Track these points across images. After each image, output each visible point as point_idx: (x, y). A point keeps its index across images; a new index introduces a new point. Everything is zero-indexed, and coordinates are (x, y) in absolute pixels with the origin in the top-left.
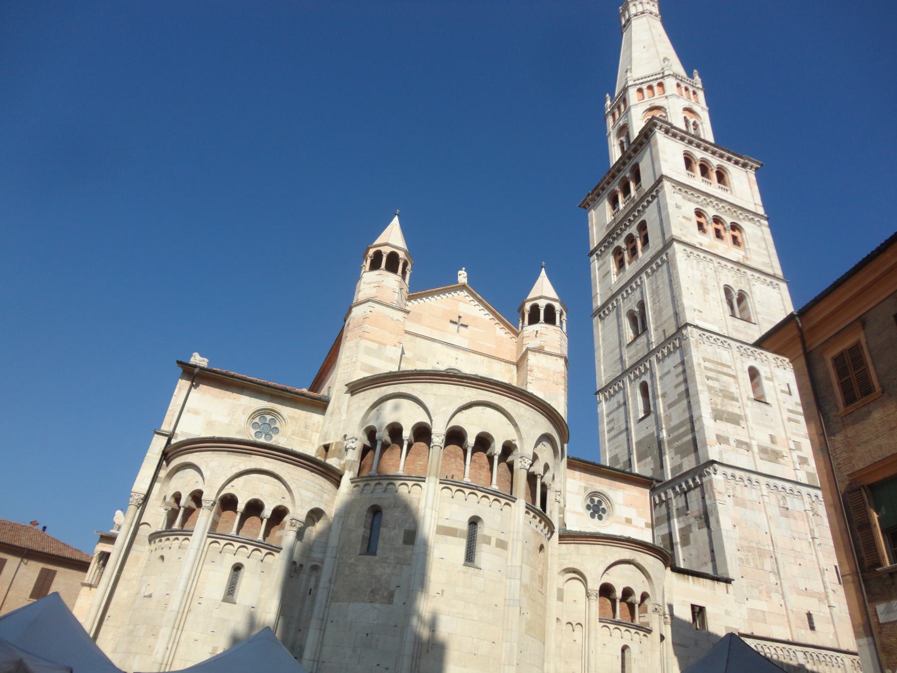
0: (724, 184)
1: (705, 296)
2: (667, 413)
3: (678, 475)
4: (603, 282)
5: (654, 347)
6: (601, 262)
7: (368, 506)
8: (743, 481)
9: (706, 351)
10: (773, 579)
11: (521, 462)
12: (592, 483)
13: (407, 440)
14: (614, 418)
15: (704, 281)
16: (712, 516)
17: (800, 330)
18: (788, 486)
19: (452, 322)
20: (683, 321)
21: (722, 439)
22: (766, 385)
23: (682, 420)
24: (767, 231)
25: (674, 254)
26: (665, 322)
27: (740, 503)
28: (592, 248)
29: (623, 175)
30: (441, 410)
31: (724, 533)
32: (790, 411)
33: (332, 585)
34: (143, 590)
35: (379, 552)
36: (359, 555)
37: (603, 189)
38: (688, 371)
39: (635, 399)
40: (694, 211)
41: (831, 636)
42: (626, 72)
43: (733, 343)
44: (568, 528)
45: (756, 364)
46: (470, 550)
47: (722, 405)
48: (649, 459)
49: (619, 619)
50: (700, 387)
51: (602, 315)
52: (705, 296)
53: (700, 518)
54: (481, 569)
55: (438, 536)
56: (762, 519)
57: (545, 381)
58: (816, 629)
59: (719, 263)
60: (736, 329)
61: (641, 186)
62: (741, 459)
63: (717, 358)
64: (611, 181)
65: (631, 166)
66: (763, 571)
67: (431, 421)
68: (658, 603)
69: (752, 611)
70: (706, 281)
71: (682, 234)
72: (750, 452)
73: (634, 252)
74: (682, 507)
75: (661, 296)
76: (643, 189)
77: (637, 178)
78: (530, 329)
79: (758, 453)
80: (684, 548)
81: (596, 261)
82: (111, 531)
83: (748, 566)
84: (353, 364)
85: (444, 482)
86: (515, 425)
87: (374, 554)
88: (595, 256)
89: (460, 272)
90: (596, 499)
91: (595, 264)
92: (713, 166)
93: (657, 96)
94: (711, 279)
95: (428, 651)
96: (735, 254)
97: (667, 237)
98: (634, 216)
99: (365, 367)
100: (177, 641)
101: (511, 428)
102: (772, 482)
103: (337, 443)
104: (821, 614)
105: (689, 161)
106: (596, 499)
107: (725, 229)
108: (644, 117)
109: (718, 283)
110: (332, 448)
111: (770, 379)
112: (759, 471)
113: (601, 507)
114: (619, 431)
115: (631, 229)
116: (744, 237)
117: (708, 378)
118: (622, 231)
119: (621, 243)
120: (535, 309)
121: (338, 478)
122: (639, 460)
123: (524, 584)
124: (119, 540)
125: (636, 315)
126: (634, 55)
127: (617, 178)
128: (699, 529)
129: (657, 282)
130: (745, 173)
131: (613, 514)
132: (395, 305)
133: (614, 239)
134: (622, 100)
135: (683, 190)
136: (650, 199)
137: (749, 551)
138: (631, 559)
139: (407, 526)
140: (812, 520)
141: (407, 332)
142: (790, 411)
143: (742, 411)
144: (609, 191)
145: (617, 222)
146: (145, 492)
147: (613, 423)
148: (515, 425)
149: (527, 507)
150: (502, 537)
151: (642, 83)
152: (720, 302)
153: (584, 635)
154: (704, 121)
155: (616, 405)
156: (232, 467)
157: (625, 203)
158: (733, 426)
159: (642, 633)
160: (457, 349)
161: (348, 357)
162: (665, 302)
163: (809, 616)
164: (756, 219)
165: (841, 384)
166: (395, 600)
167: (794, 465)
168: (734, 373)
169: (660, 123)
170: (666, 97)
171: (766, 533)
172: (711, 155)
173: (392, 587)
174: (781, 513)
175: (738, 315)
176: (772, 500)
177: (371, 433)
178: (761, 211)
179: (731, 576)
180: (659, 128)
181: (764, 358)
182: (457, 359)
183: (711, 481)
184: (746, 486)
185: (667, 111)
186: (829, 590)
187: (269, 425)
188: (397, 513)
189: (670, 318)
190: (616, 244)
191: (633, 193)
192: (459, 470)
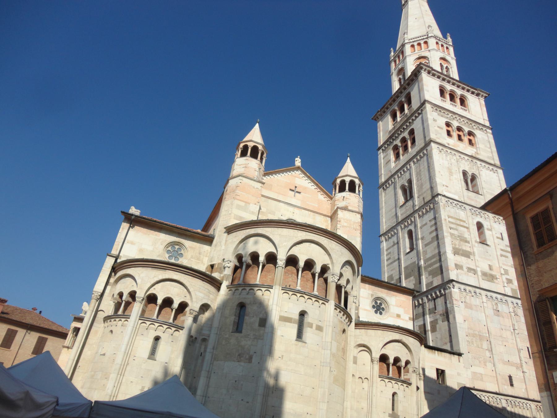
0: (465, 106)
1: (450, 177)
2: (425, 249)
3: (430, 288)
5: (417, 208)
6: (385, 154)
7: (237, 303)
8: (471, 293)
9: (450, 212)
10: (488, 354)
11: (332, 278)
12: (376, 292)
13: (262, 263)
14: (390, 252)
15: (450, 167)
16: (451, 314)
17: (510, 199)
18: (499, 296)
19: (291, 190)
20: (436, 192)
21: (458, 267)
22: (487, 233)
23: (433, 254)
24: (491, 136)
25: (431, 150)
26: (425, 192)
27: (469, 306)
28: (379, 145)
29: (400, 100)
30: (284, 244)
31: (458, 325)
32: (502, 250)
33: (215, 350)
34: (100, 351)
35: (243, 331)
36: (232, 332)
37: (387, 108)
38: (438, 224)
39: (404, 240)
40: (444, 123)
41: (523, 390)
42: (404, 34)
43: (467, 207)
44: (361, 319)
45: (481, 220)
46: (300, 331)
47: (459, 245)
48: (412, 278)
49: (391, 376)
50: (445, 234)
51: (385, 187)
52: (450, 177)
53: (444, 315)
54: (306, 343)
55: (280, 322)
56: (482, 317)
57: (348, 228)
58: (514, 385)
59: (460, 156)
60: (469, 198)
61: (411, 107)
62: (471, 280)
63: (457, 216)
64: (392, 103)
66: (482, 349)
67: (277, 251)
68: (416, 367)
69: (474, 373)
70: (451, 167)
71: (437, 138)
72: (476, 275)
73: (406, 148)
74: (432, 308)
75: (422, 176)
77: (409, 102)
78: (339, 195)
79: (481, 276)
80: (433, 334)
81: (382, 154)
82: (81, 315)
83: (472, 346)
85: (284, 289)
86: (329, 255)
87: (241, 332)
88: (381, 151)
89: (296, 159)
90: (379, 302)
91: (381, 155)
92: (458, 94)
93: (423, 50)
94: (454, 166)
95: (273, 392)
96: (470, 151)
97: (427, 139)
98: (407, 126)
99: (236, 217)
100: (120, 382)
101: (327, 257)
102: (489, 294)
103: (219, 264)
104: (517, 376)
105: (442, 92)
106: (379, 302)
107: (464, 135)
108: (415, 63)
109: (459, 169)
110: (216, 266)
111: (490, 230)
112: (481, 287)
113: (381, 307)
114: (394, 260)
115: (405, 134)
116: (476, 140)
117: (451, 228)
118: (399, 135)
119: (398, 142)
120: (343, 183)
121: (219, 285)
122: (406, 278)
123: (333, 353)
124: (86, 320)
125: (406, 188)
126: (409, 23)
127: (395, 102)
128: (442, 322)
129: (420, 167)
130: (478, 99)
131: (389, 311)
132: (256, 179)
133: (393, 140)
134: (401, 51)
135: (438, 110)
136: (417, 115)
137: (473, 336)
138: (400, 339)
139: (261, 316)
140: (513, 318)
141: (263, 196)
142: (502, 250)
143: (472, 249)
144: (391, 109)
145: (396, 129)
146: (101, 291)
147: (390, 254)
148: (329, 255)
149: (335, 306)
150: (320, 324)
151: (414, 42)
152: (459, 180)
153: (369, 386)
154: (453, 66)
155: (392, 244)
156: (155, 277)
157: (401, 117)
158: (466, 258)
159: (405, 385)
160: (294, 207)
162: (424, 180)
163: (510, 377)
164: (484, 129)
165: (536, 234)
166: (253, 360)
167: (504, 284)
168: (467, 225)
169: (424, 67)
170: (429, 51)
171: (485, 326)
172: (457, 88)
173: (252, 353)
174: (494, 313)
175: (471, 189)
176: (489, 305)
177: (240, 258)
178: (487, 124)
179: (462, 352)
180: (424, 70)
181: (487, 217)
182: (294, 213)
183: (451, 293)
184: (473, 296)
185: (429, 60)
186: (523, 362)
187: (177, 252)
188: (255, 308)
189: (428, 190)
190: (395, 143)
191: (406, 111)
192: (294, 282)
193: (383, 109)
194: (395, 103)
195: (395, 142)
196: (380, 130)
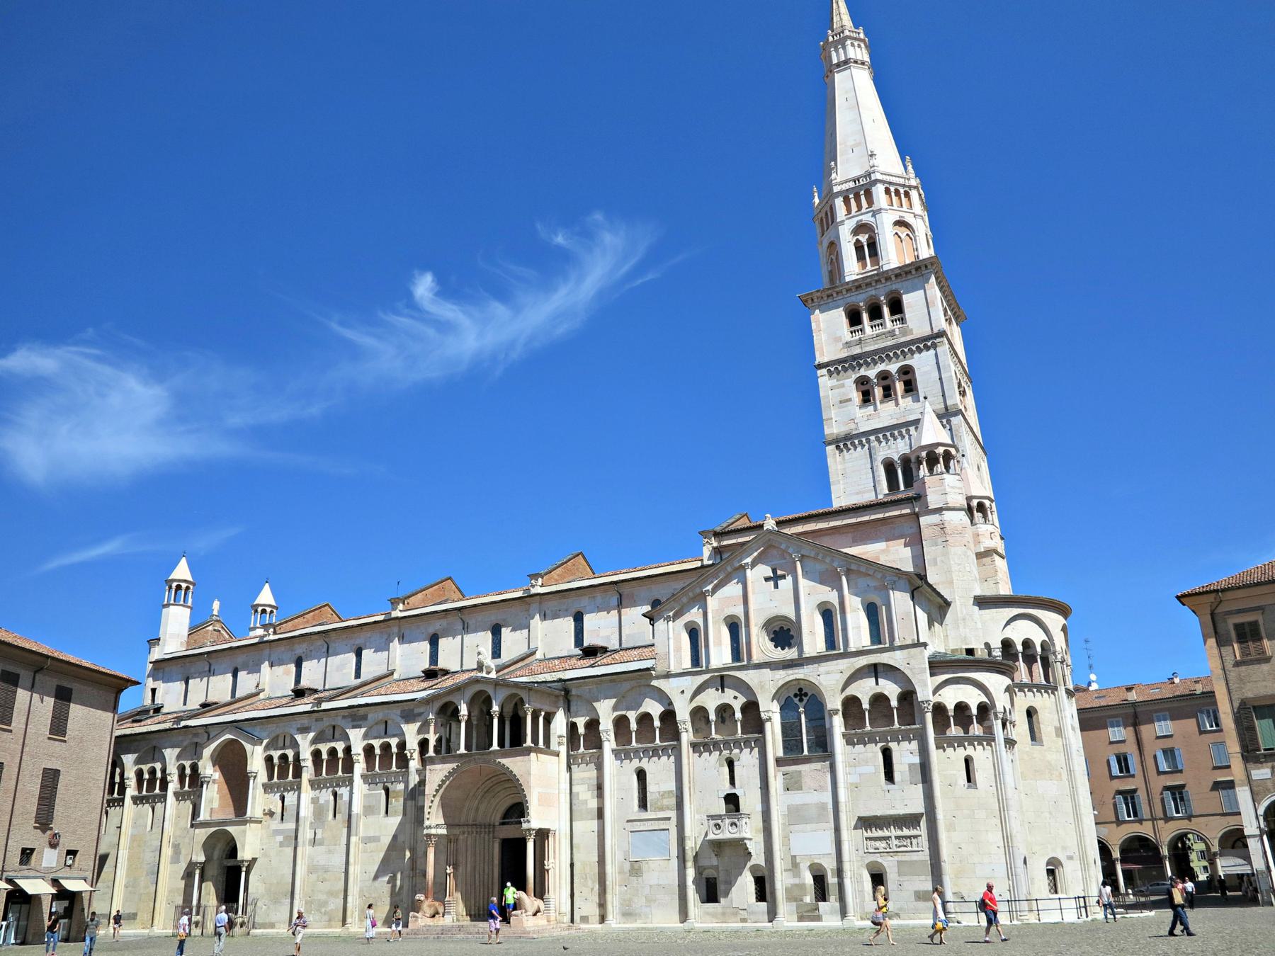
4: (839, 408)
6: (833, 382)
29: (873, 293)
35: (1044, 743)
37: (837, 293)
51: (842, 446)
61: (903, 320)
64: (853, 290)
65: (888, 289)
73: (888, 393)
76: (910, 327)
81: (827, 377)
84: (969, 574)
88: (824, 371)
93: (905, 208)
118: (875, 364)
119: (872, 373)
127: (861, 291)
133: (860, 366)
136: (921, 346)
151: (890, 183)
161: (959, 564)
177: (1007, 645)
190: (863, 372)
193: (830, 291)
194: (858, 292)
195: (865, 371)
196: (818, 325)
